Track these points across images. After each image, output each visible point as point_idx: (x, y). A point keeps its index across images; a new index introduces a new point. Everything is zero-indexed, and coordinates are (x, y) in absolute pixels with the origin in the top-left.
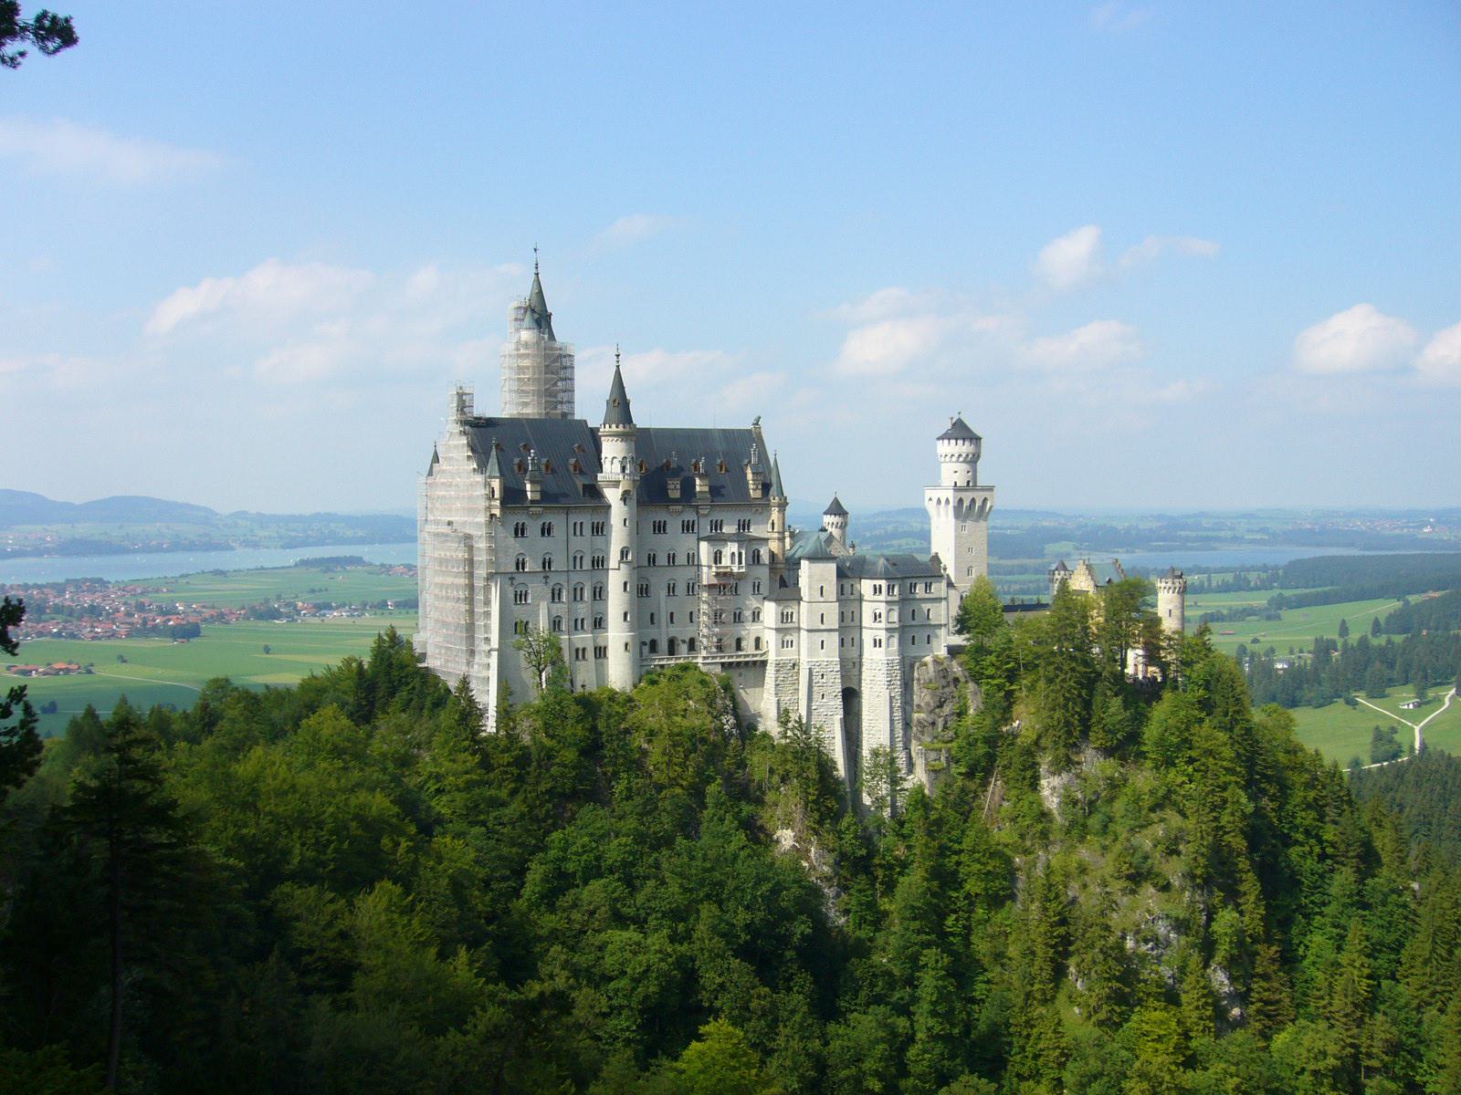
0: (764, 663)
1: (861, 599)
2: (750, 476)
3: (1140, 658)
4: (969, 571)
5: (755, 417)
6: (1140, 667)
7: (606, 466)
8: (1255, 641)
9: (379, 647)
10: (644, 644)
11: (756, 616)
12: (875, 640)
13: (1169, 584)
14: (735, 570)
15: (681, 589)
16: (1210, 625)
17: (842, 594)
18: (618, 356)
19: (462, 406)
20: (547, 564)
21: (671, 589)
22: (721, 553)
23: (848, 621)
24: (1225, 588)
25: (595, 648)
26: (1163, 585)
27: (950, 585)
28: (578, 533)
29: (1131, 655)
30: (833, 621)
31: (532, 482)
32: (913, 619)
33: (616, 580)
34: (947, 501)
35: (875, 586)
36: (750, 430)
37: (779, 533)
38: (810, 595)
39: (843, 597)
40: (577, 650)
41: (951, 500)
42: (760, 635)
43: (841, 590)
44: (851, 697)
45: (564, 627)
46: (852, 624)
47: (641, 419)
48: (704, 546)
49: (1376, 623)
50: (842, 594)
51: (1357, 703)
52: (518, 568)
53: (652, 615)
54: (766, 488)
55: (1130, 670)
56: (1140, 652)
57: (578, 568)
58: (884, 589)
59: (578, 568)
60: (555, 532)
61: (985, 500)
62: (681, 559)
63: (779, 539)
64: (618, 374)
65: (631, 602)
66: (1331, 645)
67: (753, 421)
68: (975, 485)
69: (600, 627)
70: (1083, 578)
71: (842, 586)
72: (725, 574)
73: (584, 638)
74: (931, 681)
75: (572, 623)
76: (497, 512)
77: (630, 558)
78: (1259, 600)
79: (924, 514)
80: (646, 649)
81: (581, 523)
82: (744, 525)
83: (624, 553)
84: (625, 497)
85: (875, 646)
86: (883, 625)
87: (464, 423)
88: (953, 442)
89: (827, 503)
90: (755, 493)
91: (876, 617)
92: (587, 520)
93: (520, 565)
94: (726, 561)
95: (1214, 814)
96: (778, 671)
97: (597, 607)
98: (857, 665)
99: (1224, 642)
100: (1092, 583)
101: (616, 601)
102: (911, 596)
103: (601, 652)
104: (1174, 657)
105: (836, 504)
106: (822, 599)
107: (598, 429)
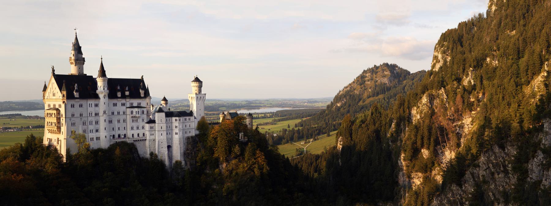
0: (145, 140)
1: (172, 123)
2: (141, 91)
3: (243, 135)
4: (200, 115)
6: (243, 137)
7: (99, 89)
8: (269, 130)
9: (28, 139)
10: (111, 136)
11: (143, 128)
12: (176, 133)
13: (249, 117)
14: (137, 116)
15: (122, 121)
16: (258, 126)
18: (102, 59)
19: (53, 71)
20: (81, 115)
21: (119, 121)
22: (133, 111)
23: (168, 128)
24: (263, 118)
25: (96, 138)
26: (248, 117)
27: (195, 118)
28: (91, 106)
29: (240, 135)
30: (164, 128)
31: (76, 92)
32: (186, 127)
33: (102, 119)
34: (194, 97)
35: (175, 119)
37: (149, 106)
38: (158, 122)
39: (167, 122)
40: (91, 138)
41: (195, 97)
42: (144, 133)
44: (169, 147)
47: (109, 76)
48: (128, 109)
49: (296, 125)
51: (292, 143)
52: (72, 116)
53: (113, 128)
55: (240, 138)
56: (243, 133)
57: (91, 116)
58: (178, 120)
59: (91, 116)
60: (83, 106)
61: (204, 97)
62: (121, 113)
63: (149, 107)
64: (102, 64)
66: (286, 130)
67: (141, 77)
71: (167, 119)
72: (134, 117)
73: (93, 135)
74: (191, 142)
75: (89, 131)
77: (106, 113)
78: (270, 120)
79: (188, 100)
80: (112, 137)
81: (91, 104)
82: (139, 104)
83: (104, 112)
85: (176, 134)
86: (178, 129)
88: (195, 82)
89: (162, 98)
90: (142, 95)
91: (176, 127)
92: (92, 102)
93: (73, 115)
94: (134, 113)
95: (261, 171)
96: (149, 142)
97: (97, 126)
98: (171, 139)
99: (262, 130)
100: (231, 117)
101: (102, 125)
103: (98, 138)
104: (251, 134)
105: (165, 98)
106: (161, 123)
107: (96, 78)
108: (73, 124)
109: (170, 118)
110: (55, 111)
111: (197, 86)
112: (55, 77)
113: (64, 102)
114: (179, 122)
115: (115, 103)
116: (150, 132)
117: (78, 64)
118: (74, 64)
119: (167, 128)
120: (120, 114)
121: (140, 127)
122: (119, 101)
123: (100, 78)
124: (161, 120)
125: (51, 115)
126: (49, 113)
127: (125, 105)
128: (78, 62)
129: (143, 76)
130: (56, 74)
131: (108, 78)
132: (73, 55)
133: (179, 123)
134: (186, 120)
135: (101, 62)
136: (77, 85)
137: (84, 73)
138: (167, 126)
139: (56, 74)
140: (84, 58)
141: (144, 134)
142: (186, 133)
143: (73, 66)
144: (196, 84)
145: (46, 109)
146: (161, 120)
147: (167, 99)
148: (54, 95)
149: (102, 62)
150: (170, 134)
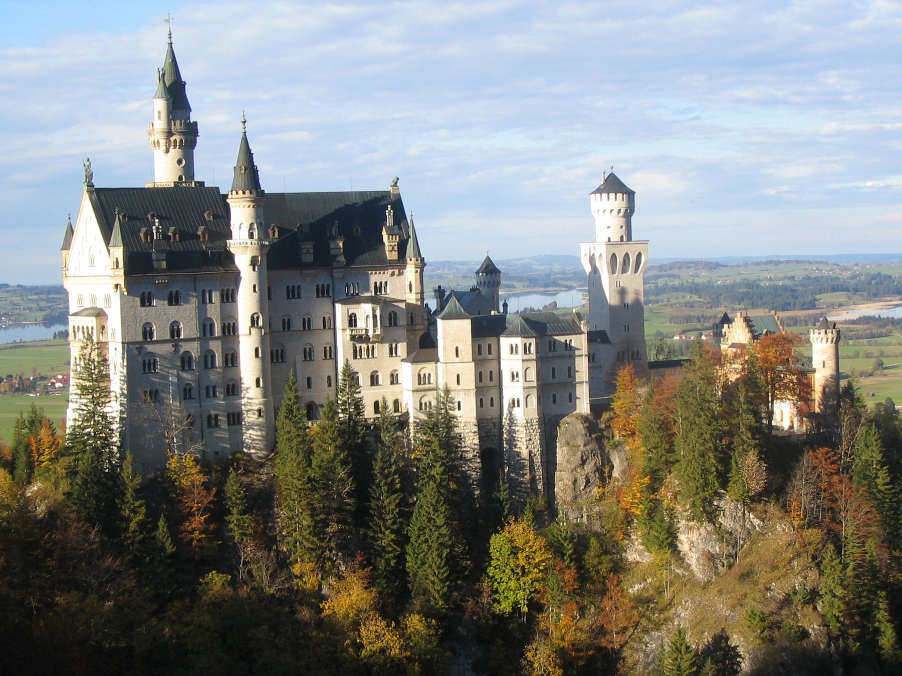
4: (627, 328)
5: (394, 179)
11: (394, 379)
14: (371, 333)
15: (319, 353)
17: (480, 353)
18: (244, 122)
19: (89, 176)
20: (175, 331)
22: (355, 316)
26: (816, 335)
34: (601, 255)
36: (389, 192)
37: (417, 293)
38: (445, 356)
39: (480, 357)
42: (399, 397)
43: (478, 352)
45: (195, 394)
46: (491, 384)
50: (480, 353)
52: (145, 337)
54: (402, 248)
58: (521, 349)
61: (639, 256)
64: (245, 141)
65: (264, 370)
68: (629, 238)
69: (233, 394)
70: (741, 332)
71: (480, 346)
72: (361, 336)
75: (204, 391)
76: (121, 281)
77: (261, 323)
84: (254, 262)
87: (90, 193)
91: (514, 376)
93: (147, 333)
94: (361, 324)
100: (749, 335)
102: (551, 354)
107: (226, 197)
108: (149, 364)
109: (492, 340)
110: (94, 319)
111: (619, 211)
112: (95, 196)
113: (117, 286)
114: (526, 357)
115: (293, 287)
116: (419, 395)
117: (175, 147)
118: (163, 147)
119: (481, 381)
120: (311, 328)
121: (384, 378)
122: (308, 279)
123: (237, 193)
124: (457, 348)
125: (83, 332)
126: (78, 327)
127: (328, 294)
128: (175, 140)
129: (398, 179)
130: (95, 187)
131: (266, 192)
132: (159, 112)
133: (523, 361)
134: (555, 350)
135: (241, 135)
136: (160, 223)
137: (196, 179)
138: (481, 373)
139: (95, 187)
140: (195, 124)
141: (396, 402)
142: (554, 401)
143: (159, 153)
144: (617, 202)
145: (71, 312)
146: (457, 348)
147: (499, 267)
148: (92, 261)
149: (245, 133)
150: (492, 405)
